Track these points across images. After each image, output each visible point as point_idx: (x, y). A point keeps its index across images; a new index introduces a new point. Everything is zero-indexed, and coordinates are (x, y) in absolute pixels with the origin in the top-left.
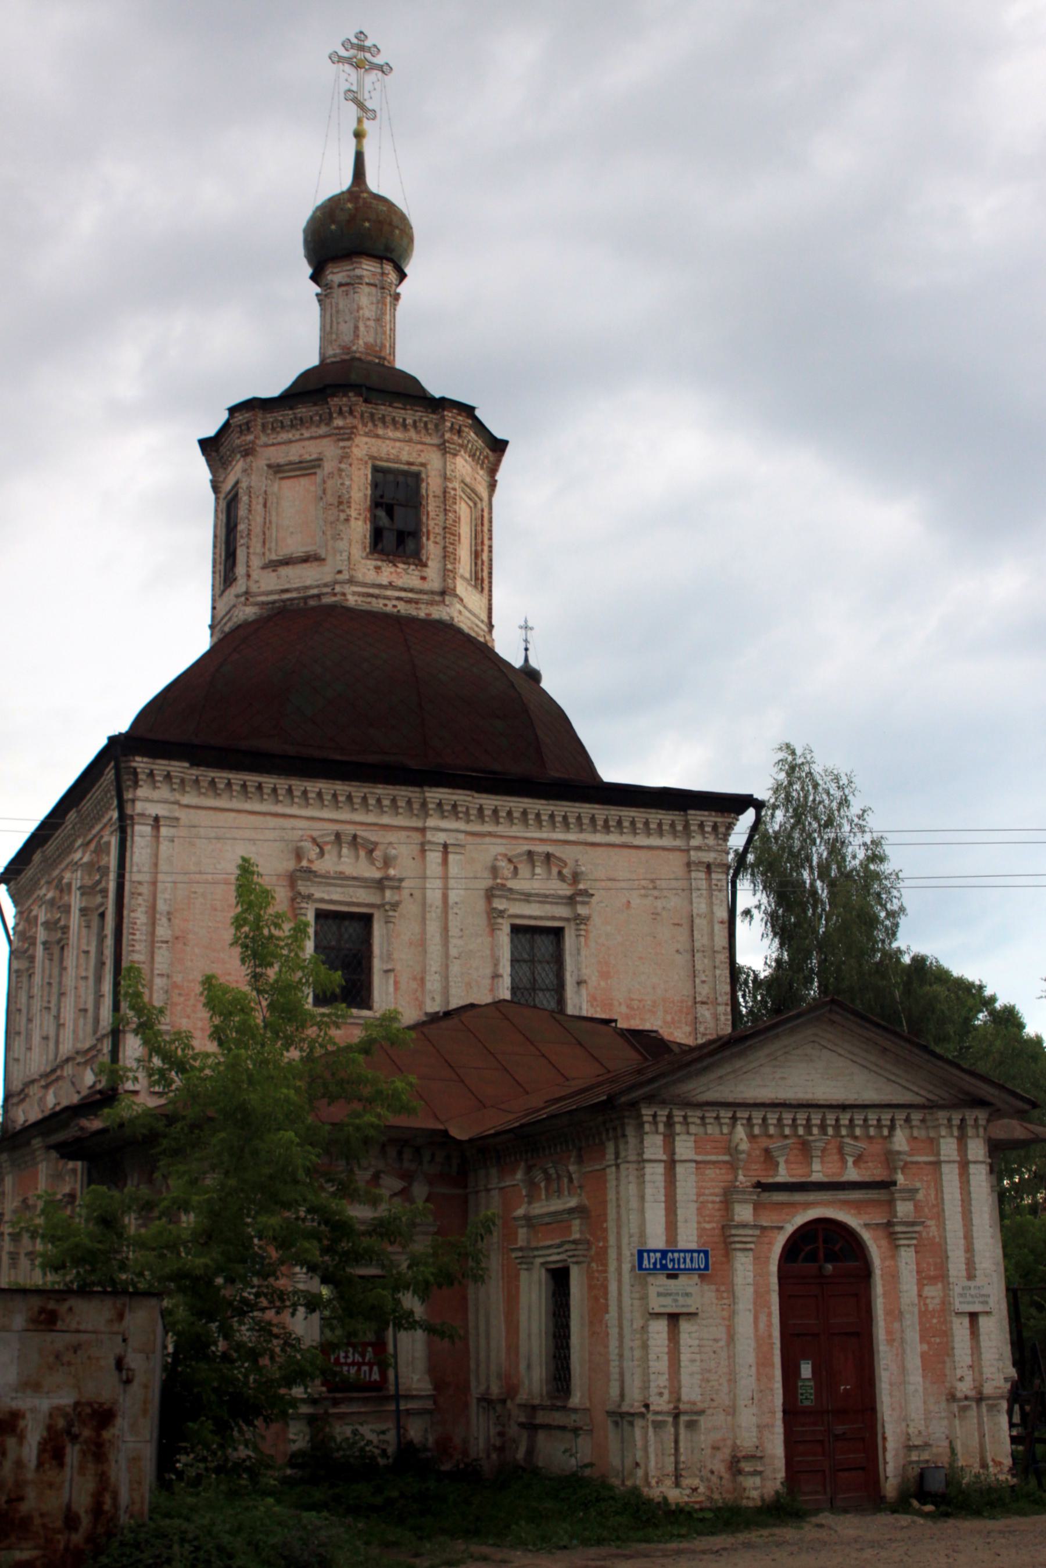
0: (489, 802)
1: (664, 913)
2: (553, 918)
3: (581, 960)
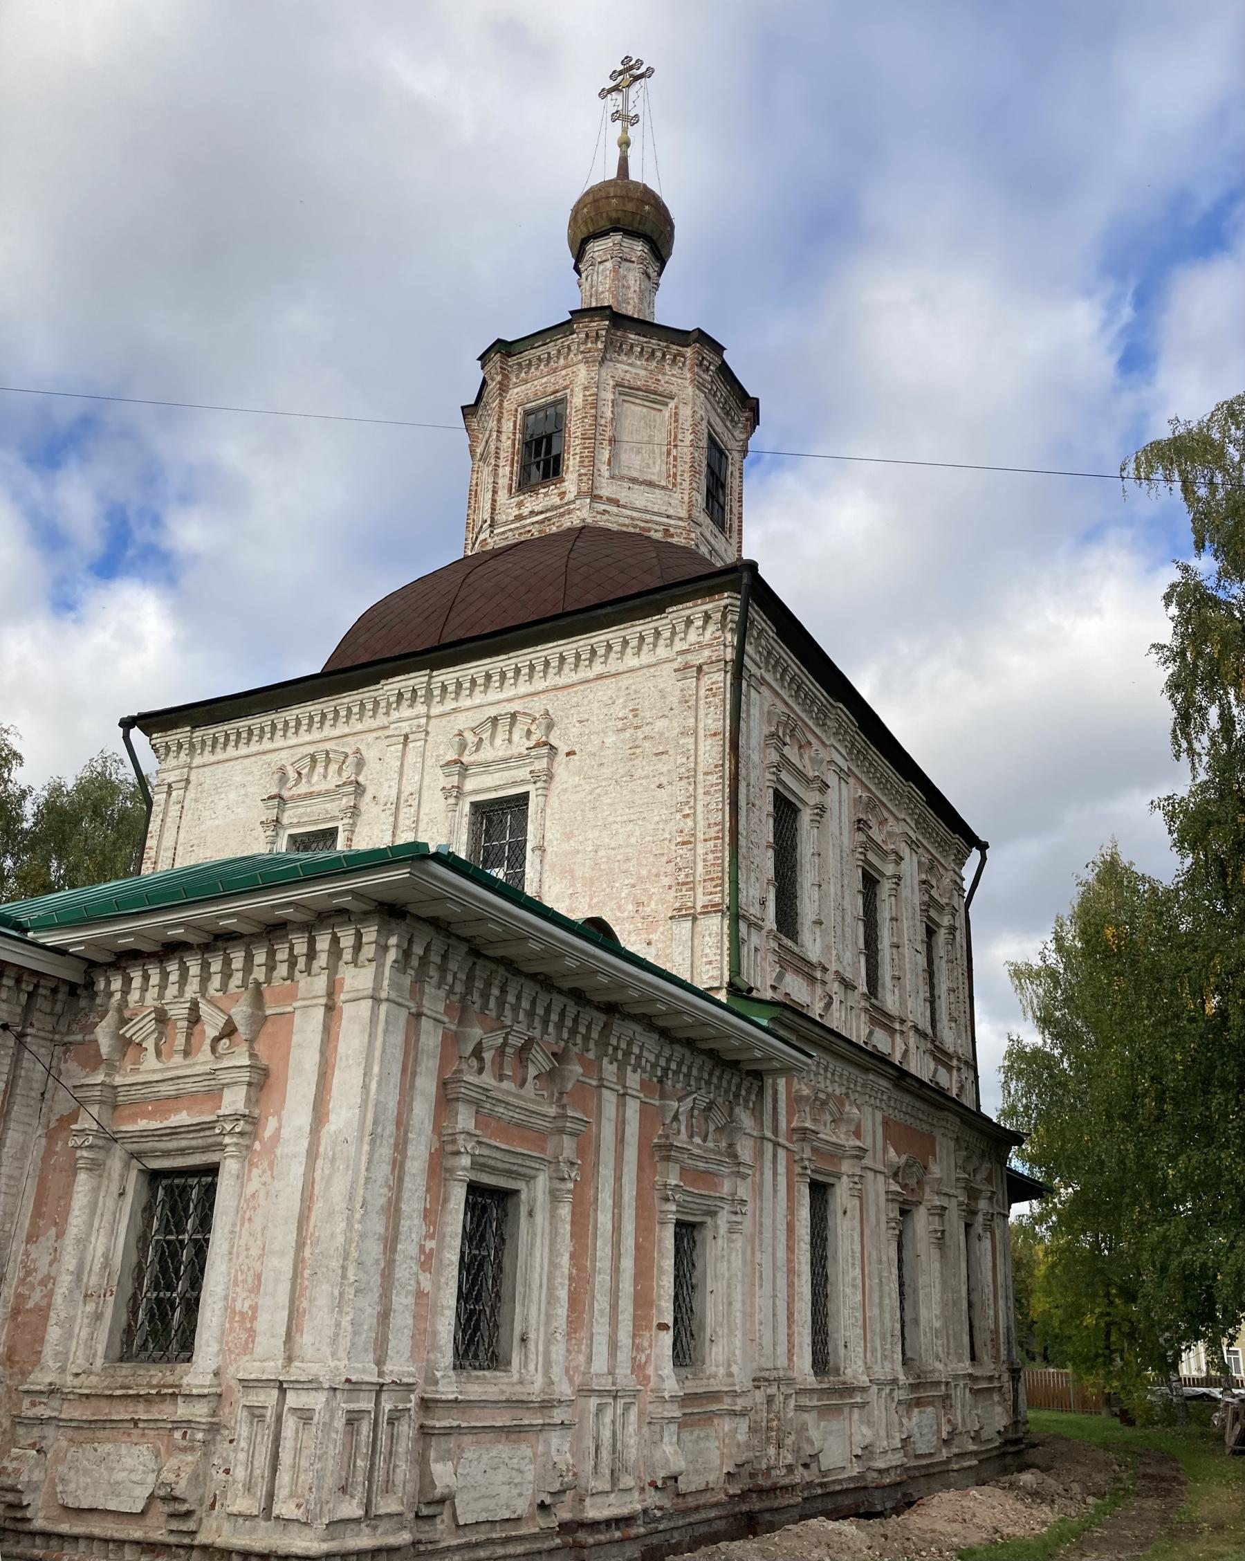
0: (447, 676)
1: (647, 744)
2: (515, 784)
3: (544, 826)
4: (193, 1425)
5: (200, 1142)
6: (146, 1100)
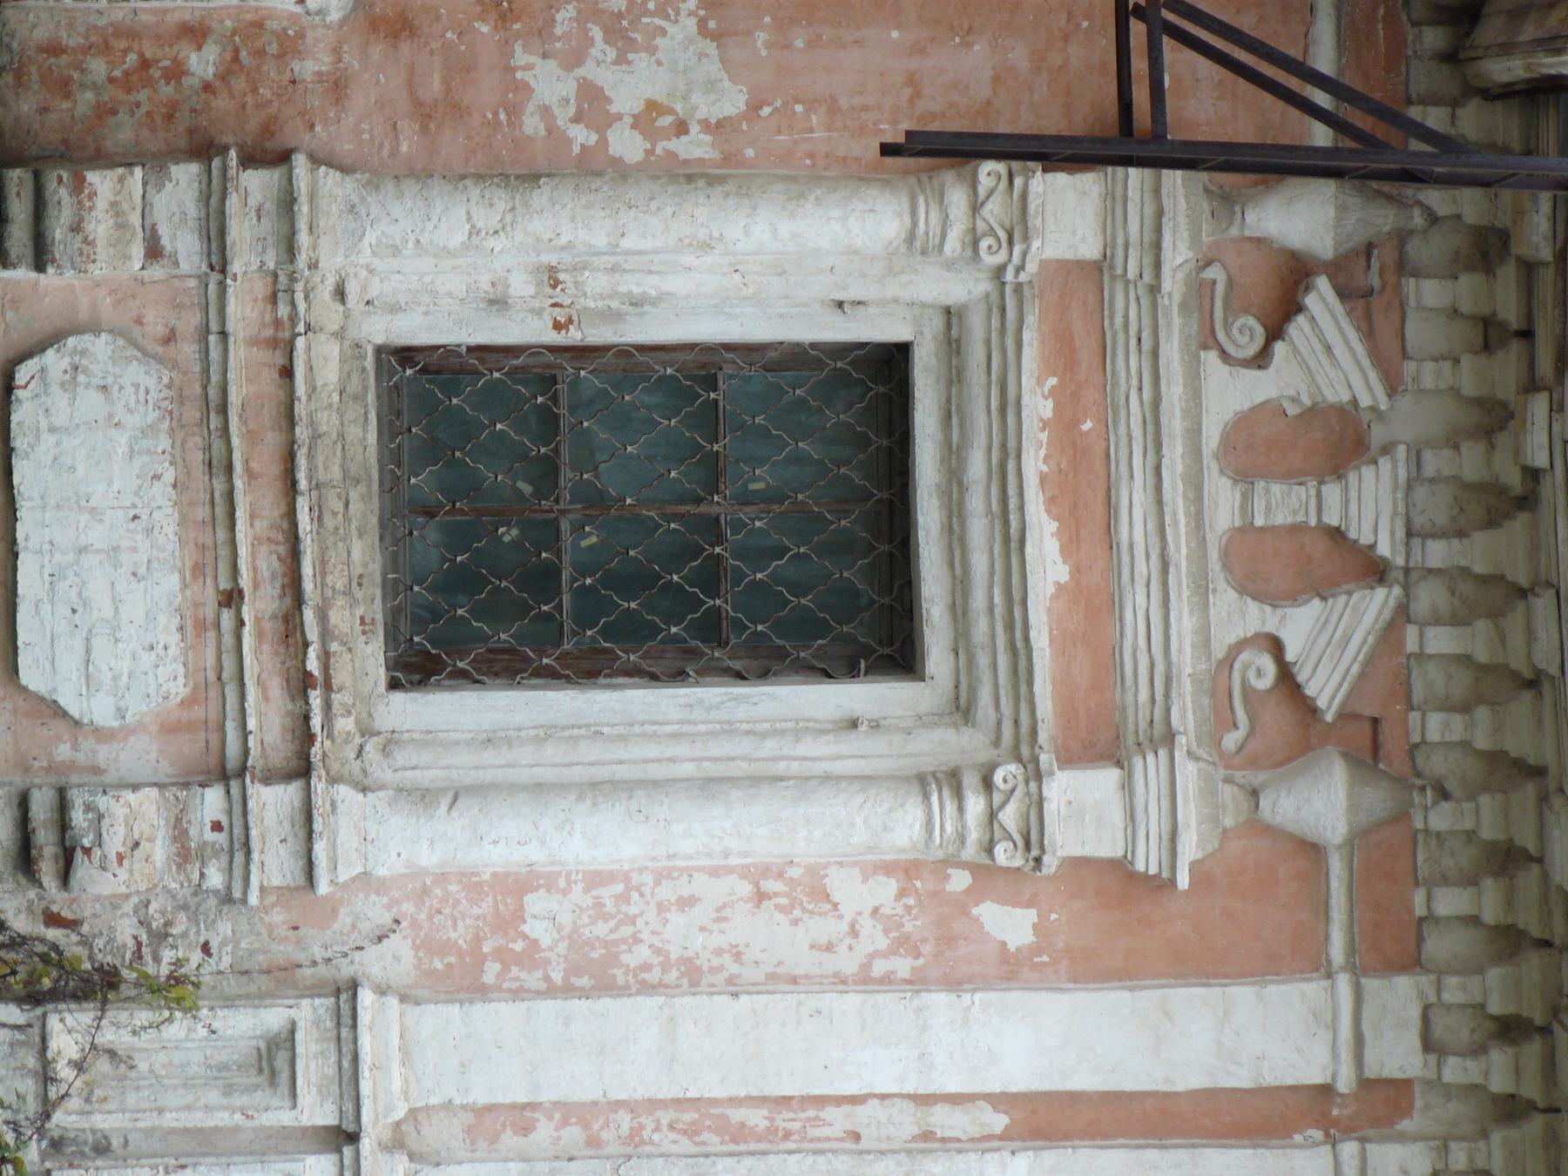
4: (239, 858)
5: (980, 627)
6: (1109, 413)
